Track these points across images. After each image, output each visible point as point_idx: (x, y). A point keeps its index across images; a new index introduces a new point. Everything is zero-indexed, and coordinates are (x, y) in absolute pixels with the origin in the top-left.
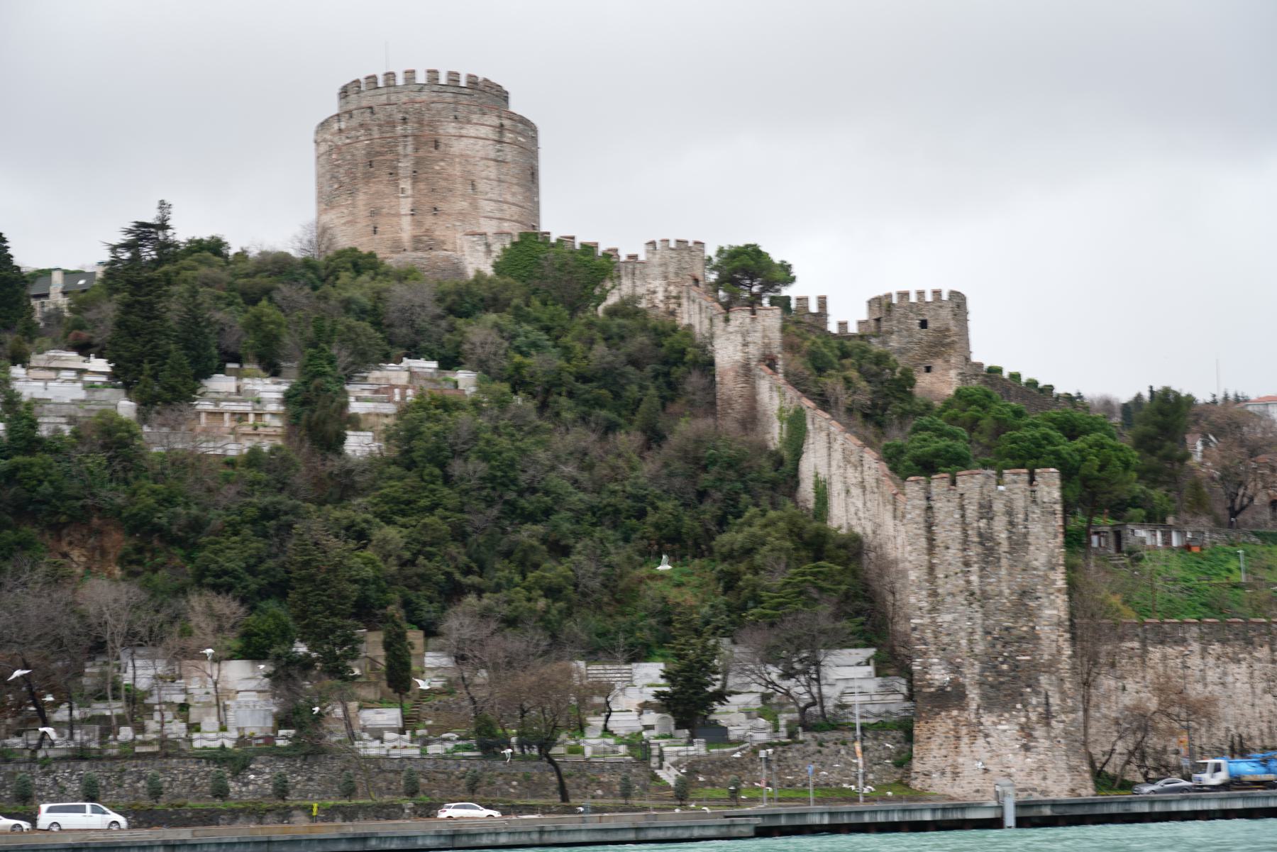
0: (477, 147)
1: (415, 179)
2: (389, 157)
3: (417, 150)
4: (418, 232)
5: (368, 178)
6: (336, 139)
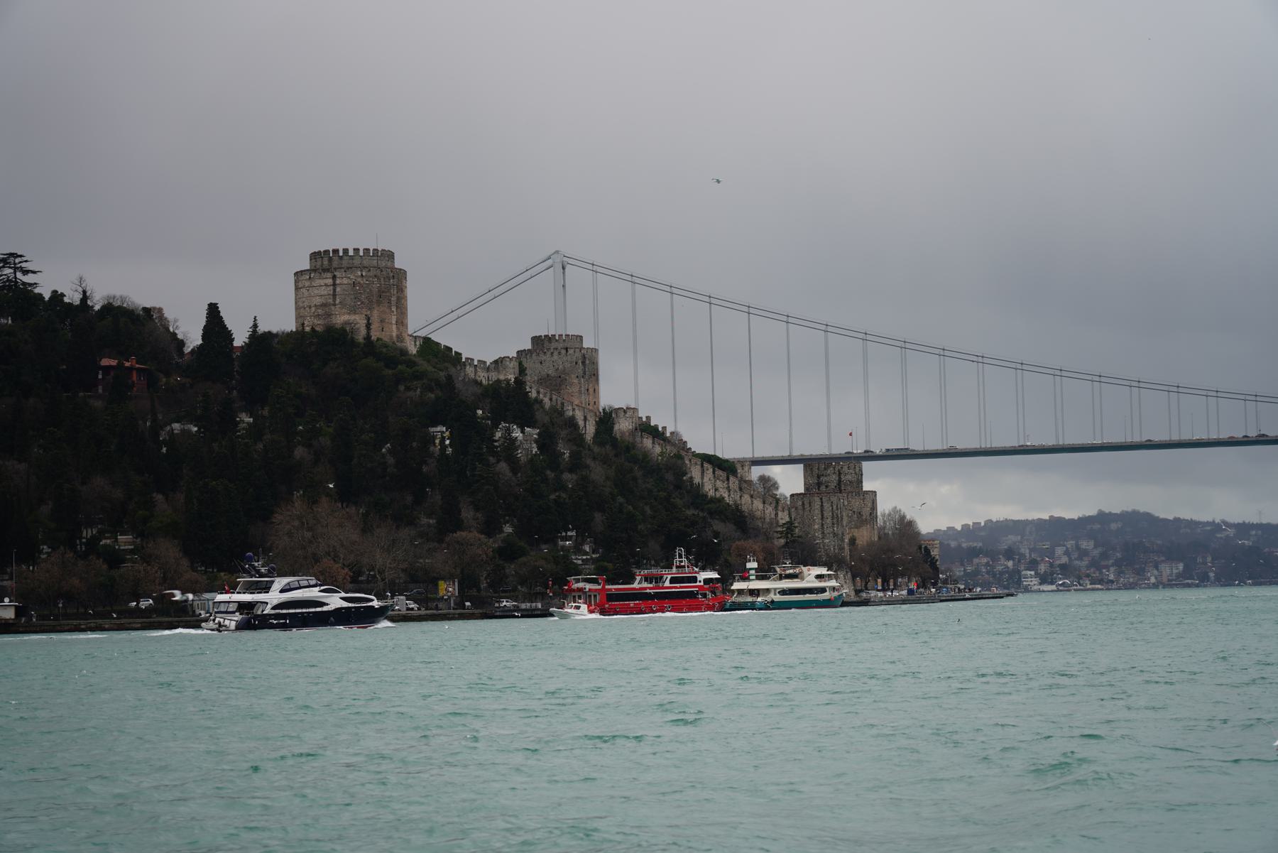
1: (397, 308)
2: (388, 294)
3: (397, 292)
4: (399, 333)
5: (379, 303)
6: (359, 280)
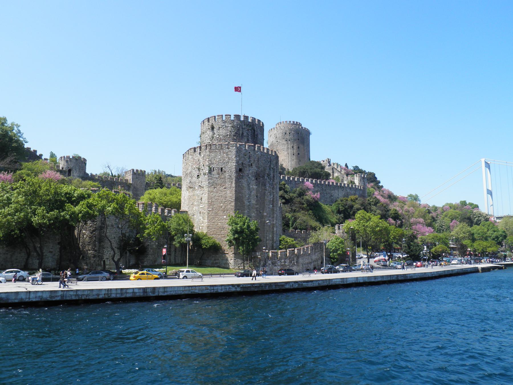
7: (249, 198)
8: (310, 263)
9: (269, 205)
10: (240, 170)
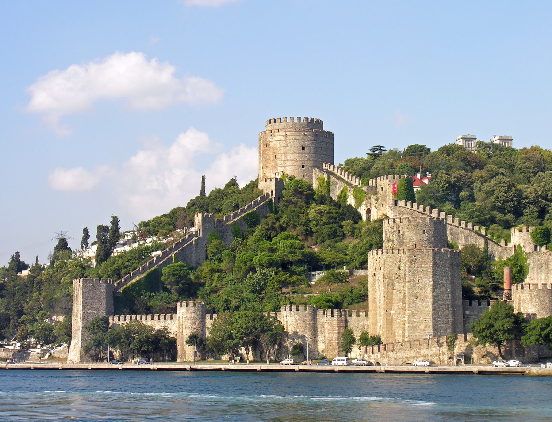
0: (278, 144)
7: (380, 300)
8: (414, 357)
9: (398, 303)
10: (375, 274)
